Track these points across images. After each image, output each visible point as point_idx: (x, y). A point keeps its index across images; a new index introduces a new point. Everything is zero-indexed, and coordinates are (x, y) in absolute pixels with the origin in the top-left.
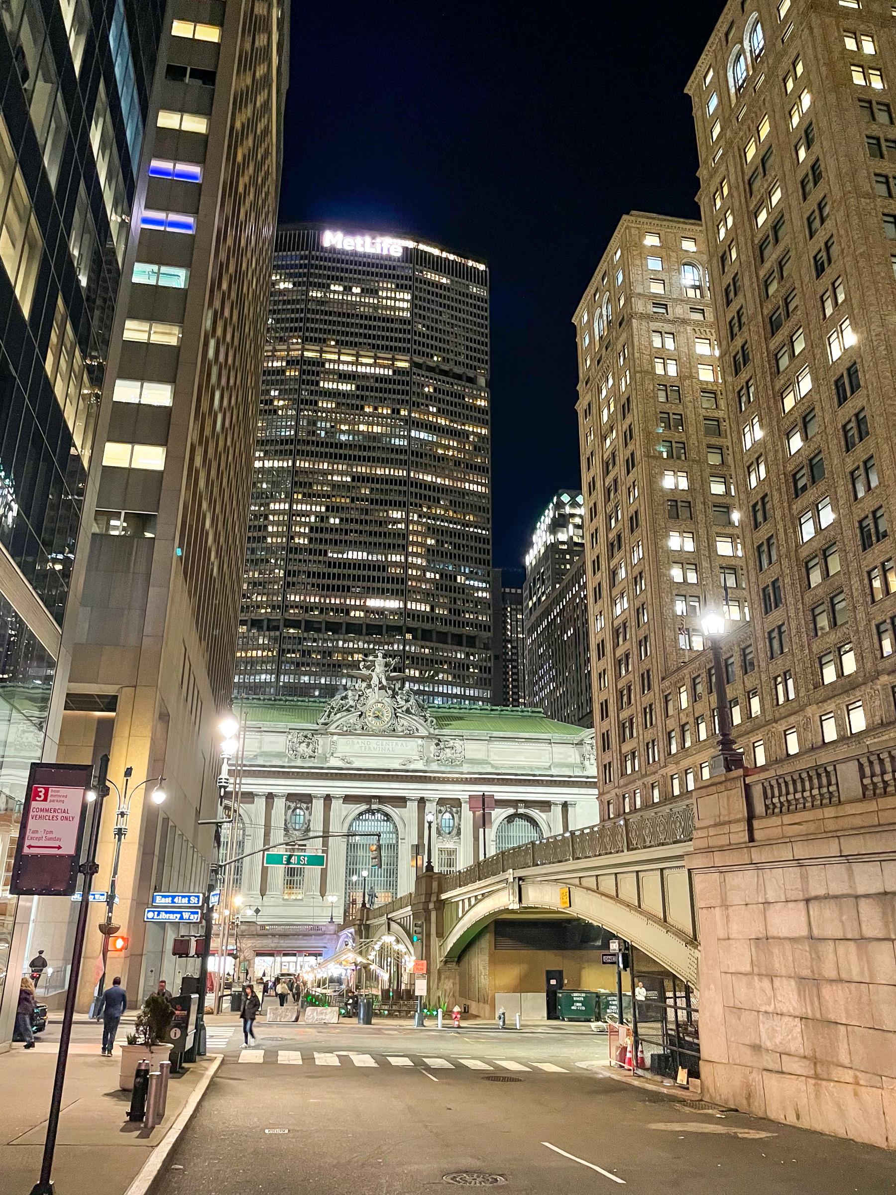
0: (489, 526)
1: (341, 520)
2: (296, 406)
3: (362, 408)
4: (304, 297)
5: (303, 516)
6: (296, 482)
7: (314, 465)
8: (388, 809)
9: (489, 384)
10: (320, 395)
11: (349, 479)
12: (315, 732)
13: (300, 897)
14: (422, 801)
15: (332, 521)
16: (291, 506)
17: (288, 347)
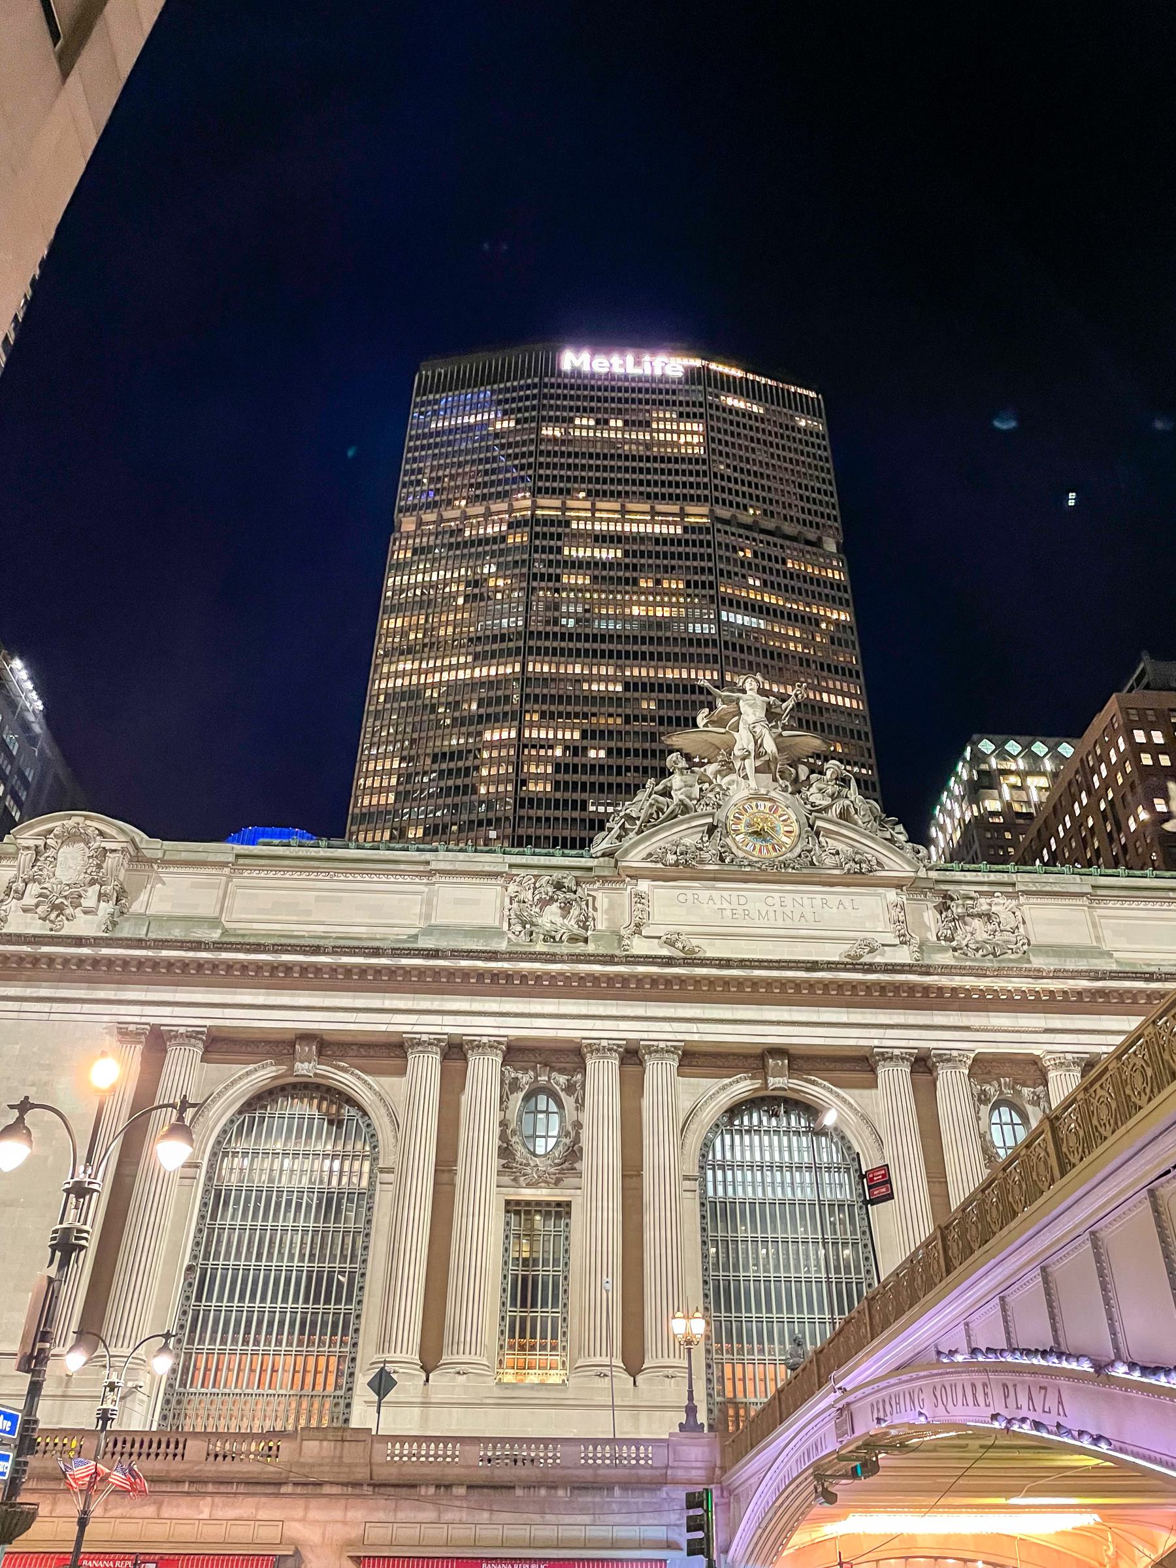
0: (872, 761)
1: (609, 752)
2: (524, 584)
3: (635, 582)
4: (533, 436)
5: (542, 747)
6: (528, 696)
7: (558, 669)
9: (842, 548)
10: (565, 566)
11: (619, 688)
13: (555, 1378)
14: (923, 1065)
15: (592, 754)
17: (511, 505)
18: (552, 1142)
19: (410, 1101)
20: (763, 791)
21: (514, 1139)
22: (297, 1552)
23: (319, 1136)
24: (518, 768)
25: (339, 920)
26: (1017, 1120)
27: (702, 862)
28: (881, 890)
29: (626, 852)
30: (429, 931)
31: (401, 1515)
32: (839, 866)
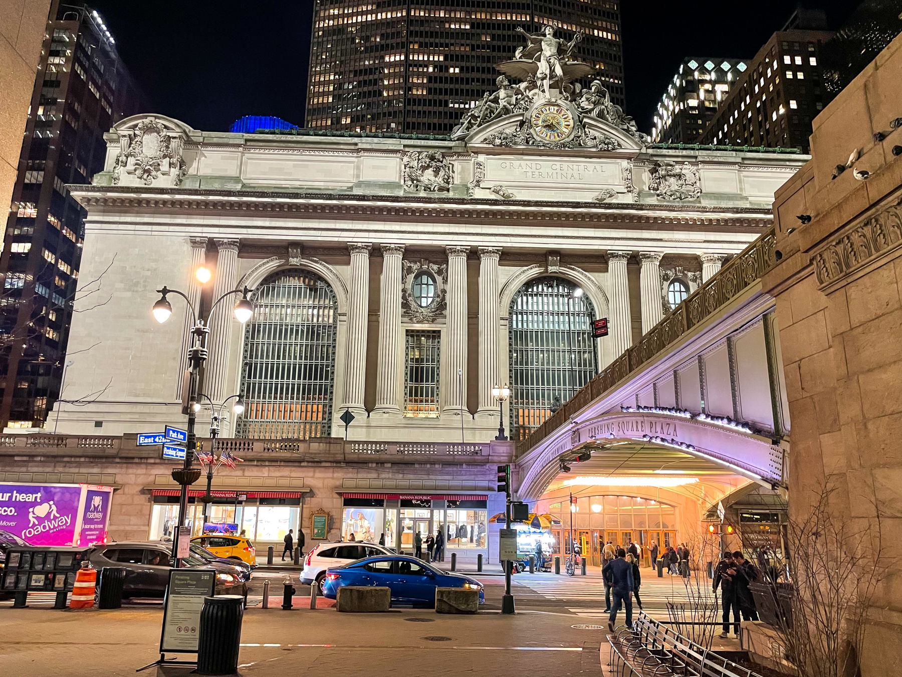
0: (622, 75)
1: (461, 70)
5: (421, 66)
6: (412, 32)
7: (429, 14)
8: (575, 274)
11: (468, 27)
12: (448, 152)
13: (433, 415)
14: (634, 260)
15: (451, 70)
16: (407, 57)
18: (430, 300)
19: (353, 278)
20: (553, 100)
21: (410, 299)
22: (311, 490)
23: (305, 297)
24: (406, 80)
25: (307, 178)
26: (683, 289)
27: (515, 143)
28: (619, 161)
29: (472, 138)
30: (359, 184)
31: (360, 476)
32: (596, 146)
